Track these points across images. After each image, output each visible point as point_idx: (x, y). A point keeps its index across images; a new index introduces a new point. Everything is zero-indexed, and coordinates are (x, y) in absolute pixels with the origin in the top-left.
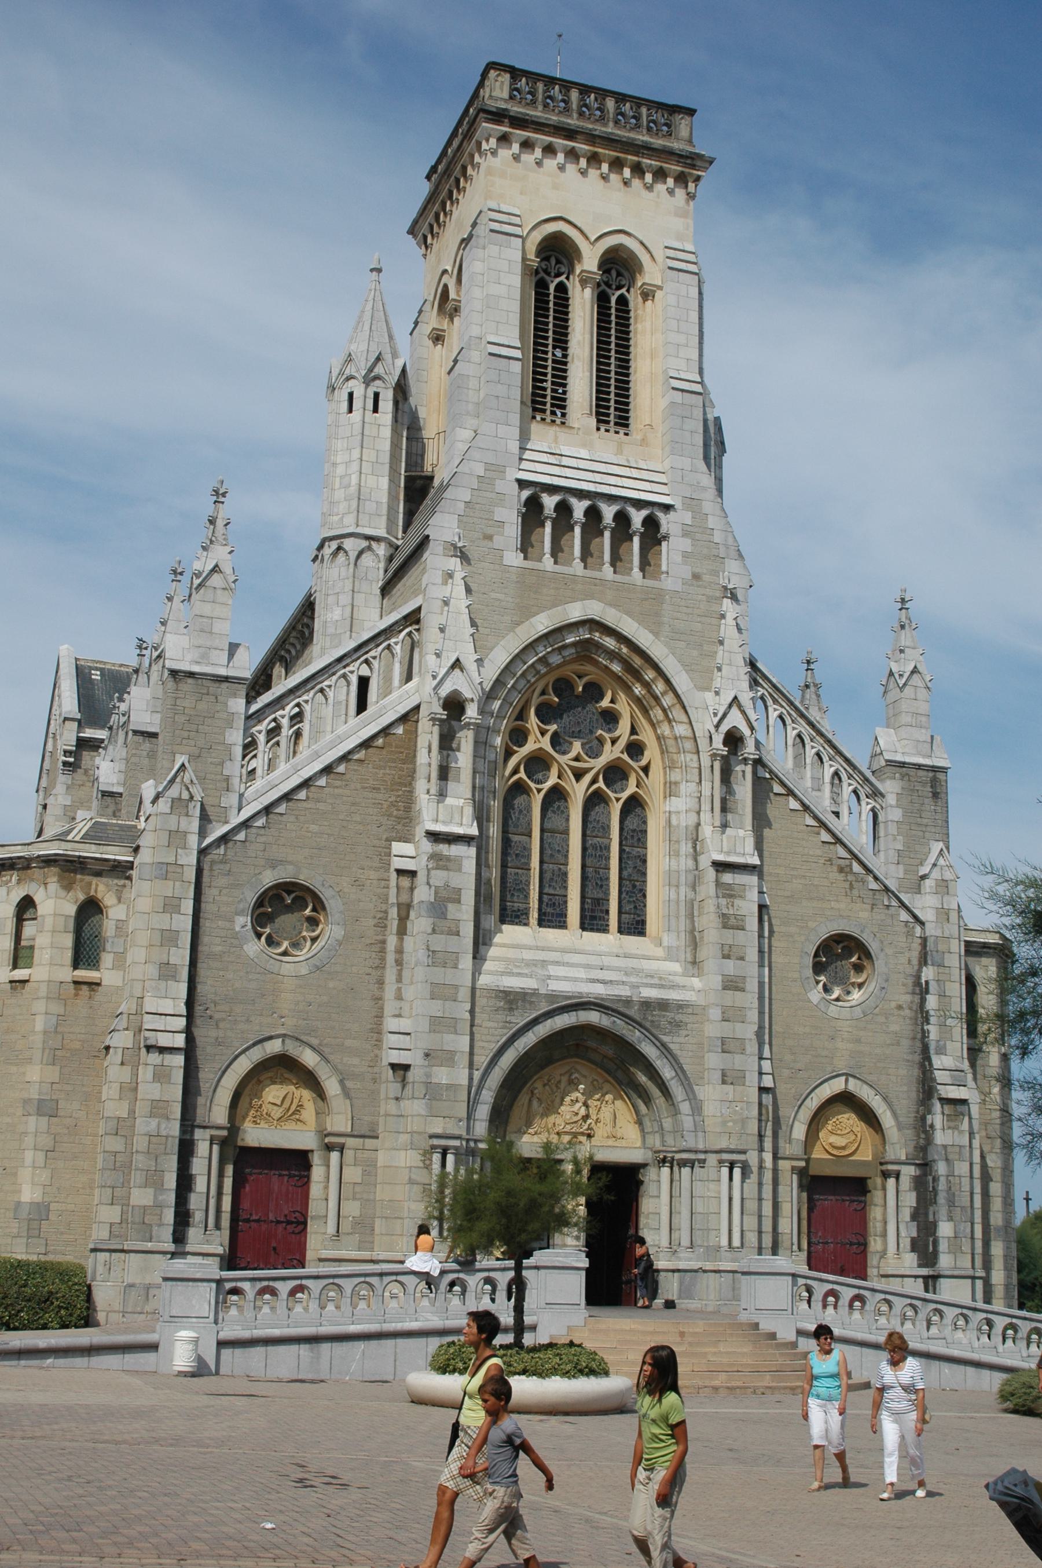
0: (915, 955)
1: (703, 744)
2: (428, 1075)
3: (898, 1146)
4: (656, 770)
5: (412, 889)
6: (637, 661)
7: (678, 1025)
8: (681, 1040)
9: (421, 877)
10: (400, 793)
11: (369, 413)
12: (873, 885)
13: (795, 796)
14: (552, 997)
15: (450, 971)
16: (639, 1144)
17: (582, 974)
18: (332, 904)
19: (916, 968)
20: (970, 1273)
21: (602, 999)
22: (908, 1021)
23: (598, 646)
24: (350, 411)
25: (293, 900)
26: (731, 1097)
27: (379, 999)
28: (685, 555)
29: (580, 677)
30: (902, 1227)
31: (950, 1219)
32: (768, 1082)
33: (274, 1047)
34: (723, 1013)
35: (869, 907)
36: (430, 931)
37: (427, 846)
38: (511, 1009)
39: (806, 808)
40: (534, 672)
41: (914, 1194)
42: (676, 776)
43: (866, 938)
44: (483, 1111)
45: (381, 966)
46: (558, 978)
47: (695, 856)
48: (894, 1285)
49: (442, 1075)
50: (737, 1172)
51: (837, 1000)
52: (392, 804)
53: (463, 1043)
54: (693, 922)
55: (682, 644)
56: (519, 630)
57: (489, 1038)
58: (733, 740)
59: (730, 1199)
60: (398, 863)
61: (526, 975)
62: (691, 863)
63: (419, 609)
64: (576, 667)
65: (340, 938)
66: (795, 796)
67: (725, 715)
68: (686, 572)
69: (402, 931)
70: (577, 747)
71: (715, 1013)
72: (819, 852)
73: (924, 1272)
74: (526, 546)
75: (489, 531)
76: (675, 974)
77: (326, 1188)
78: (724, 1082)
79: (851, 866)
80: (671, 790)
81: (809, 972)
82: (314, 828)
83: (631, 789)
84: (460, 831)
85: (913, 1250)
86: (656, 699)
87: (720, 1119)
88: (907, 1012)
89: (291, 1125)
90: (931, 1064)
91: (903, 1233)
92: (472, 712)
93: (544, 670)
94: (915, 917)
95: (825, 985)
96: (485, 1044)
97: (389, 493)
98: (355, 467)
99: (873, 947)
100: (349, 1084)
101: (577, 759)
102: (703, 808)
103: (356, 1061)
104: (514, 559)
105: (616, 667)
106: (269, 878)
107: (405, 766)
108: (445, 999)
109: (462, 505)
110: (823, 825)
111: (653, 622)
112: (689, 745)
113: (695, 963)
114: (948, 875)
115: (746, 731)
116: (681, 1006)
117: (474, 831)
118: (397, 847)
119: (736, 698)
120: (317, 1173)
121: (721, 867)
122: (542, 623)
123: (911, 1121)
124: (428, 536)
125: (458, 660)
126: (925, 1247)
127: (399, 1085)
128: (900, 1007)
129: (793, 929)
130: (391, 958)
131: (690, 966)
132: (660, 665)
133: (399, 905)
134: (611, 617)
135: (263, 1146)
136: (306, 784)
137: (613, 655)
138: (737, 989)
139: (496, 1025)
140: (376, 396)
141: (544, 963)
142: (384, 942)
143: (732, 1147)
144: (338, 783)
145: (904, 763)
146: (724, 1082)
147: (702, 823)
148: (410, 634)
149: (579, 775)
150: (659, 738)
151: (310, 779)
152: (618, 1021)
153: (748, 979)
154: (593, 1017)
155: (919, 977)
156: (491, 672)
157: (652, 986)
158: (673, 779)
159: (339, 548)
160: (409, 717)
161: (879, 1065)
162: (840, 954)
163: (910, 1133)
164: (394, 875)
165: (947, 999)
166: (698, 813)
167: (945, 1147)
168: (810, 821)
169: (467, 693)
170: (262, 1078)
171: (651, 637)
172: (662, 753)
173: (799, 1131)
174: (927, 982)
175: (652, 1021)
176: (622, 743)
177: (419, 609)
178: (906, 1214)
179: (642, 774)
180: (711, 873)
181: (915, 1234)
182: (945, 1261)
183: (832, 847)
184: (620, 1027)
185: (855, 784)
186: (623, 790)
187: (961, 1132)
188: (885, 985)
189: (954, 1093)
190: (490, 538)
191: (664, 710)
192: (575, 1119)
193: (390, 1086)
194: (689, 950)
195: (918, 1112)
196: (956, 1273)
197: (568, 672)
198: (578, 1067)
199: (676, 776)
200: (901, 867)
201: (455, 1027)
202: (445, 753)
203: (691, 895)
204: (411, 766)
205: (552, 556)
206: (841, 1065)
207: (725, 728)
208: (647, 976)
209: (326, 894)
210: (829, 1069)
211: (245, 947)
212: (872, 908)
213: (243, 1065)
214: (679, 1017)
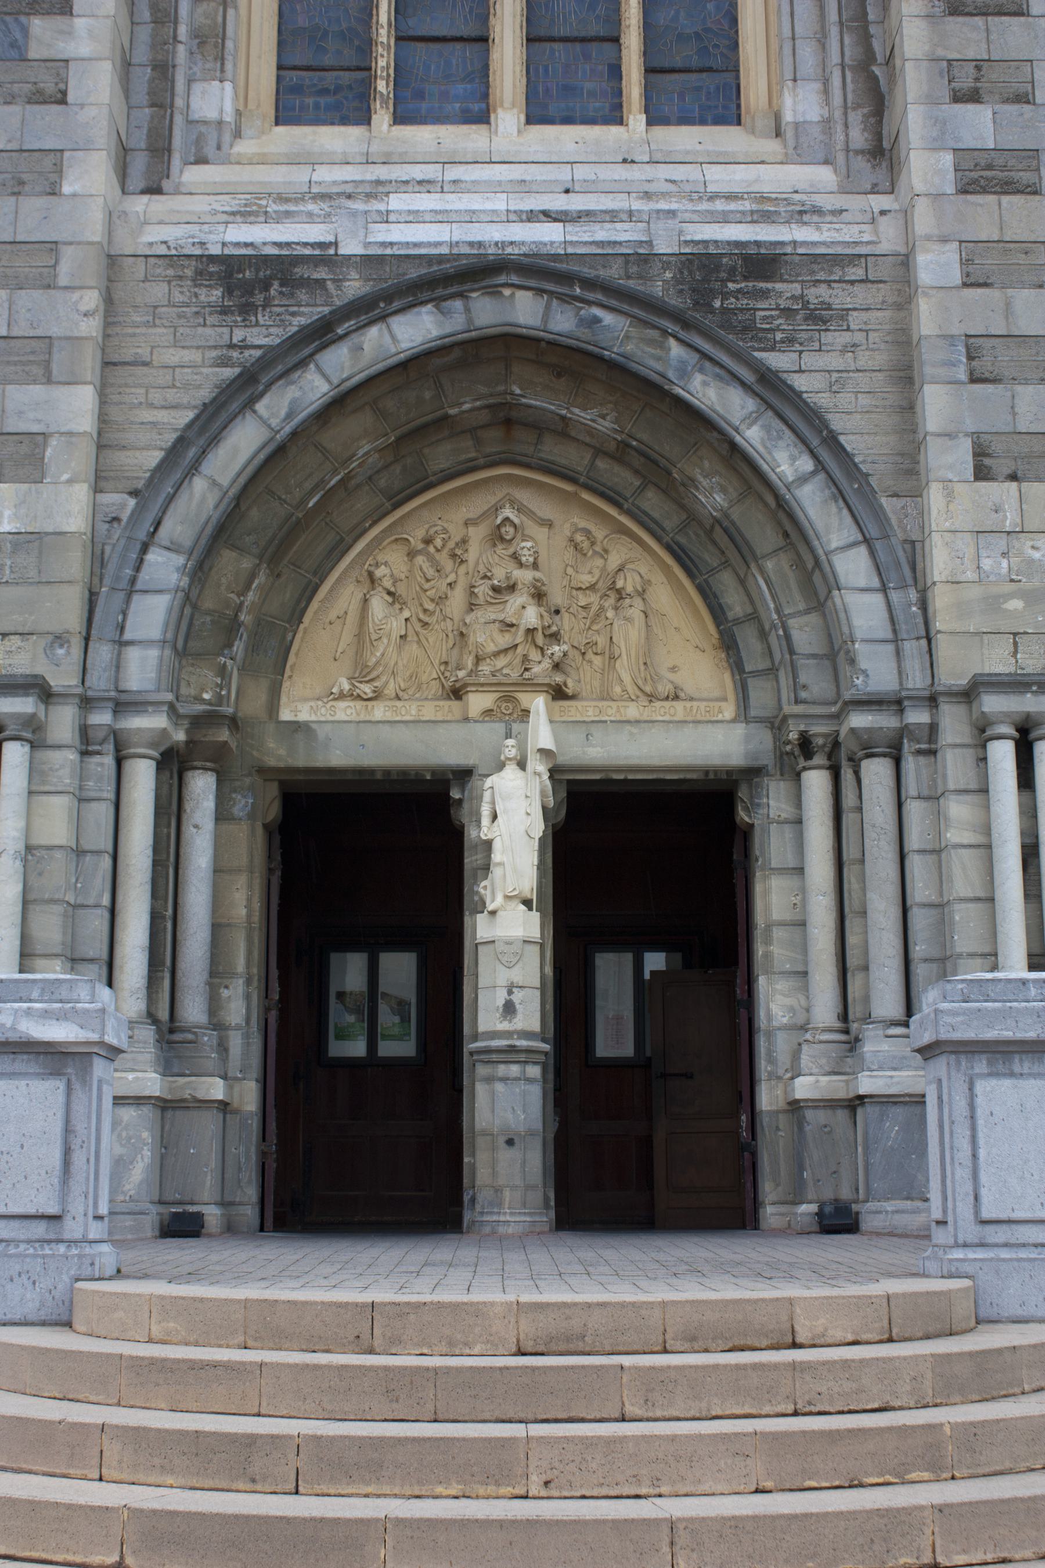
7: (819, 317)
15: (33, 205)
21: (555, 257)
26: (1010, 520)
34: (966, 262)
38: (247, 309)
44: (151, 616)
46: (415, 217)
53: (76, 407)
54: (865, 39)
57: (171, 395)
78: (982, 473)
87: (974, 593)
131: (861, 163)
139: (195, 356)
141: (378, 189)
146: (982, 473)
152: (608, 318)
154: (524, 309)
175: (724, 310)
194: (856, 118)
201: (47, 365)
214: (817, 294)
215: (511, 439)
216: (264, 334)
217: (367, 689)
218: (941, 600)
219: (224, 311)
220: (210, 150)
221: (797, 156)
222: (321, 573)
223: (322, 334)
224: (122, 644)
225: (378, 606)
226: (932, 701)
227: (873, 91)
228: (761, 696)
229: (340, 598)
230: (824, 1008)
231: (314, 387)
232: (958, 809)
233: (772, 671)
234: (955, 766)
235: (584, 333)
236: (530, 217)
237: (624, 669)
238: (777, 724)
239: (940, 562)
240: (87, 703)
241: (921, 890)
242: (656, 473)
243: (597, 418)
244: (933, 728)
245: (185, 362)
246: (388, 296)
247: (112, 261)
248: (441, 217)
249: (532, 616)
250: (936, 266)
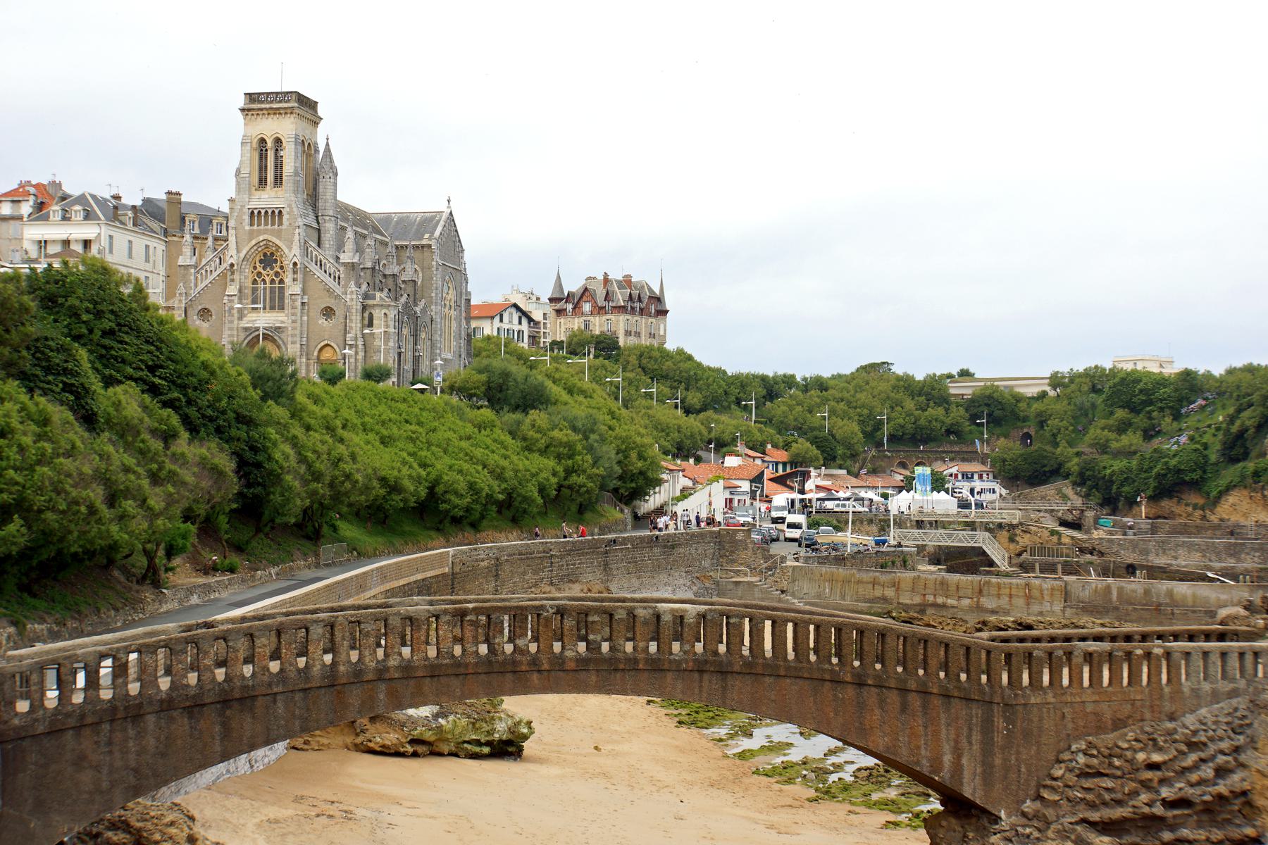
74: (252, 224)
104: (247, 228)
111: (279, 237)
122: (254, 242)
134: (270, 238)
245: (242, 335)
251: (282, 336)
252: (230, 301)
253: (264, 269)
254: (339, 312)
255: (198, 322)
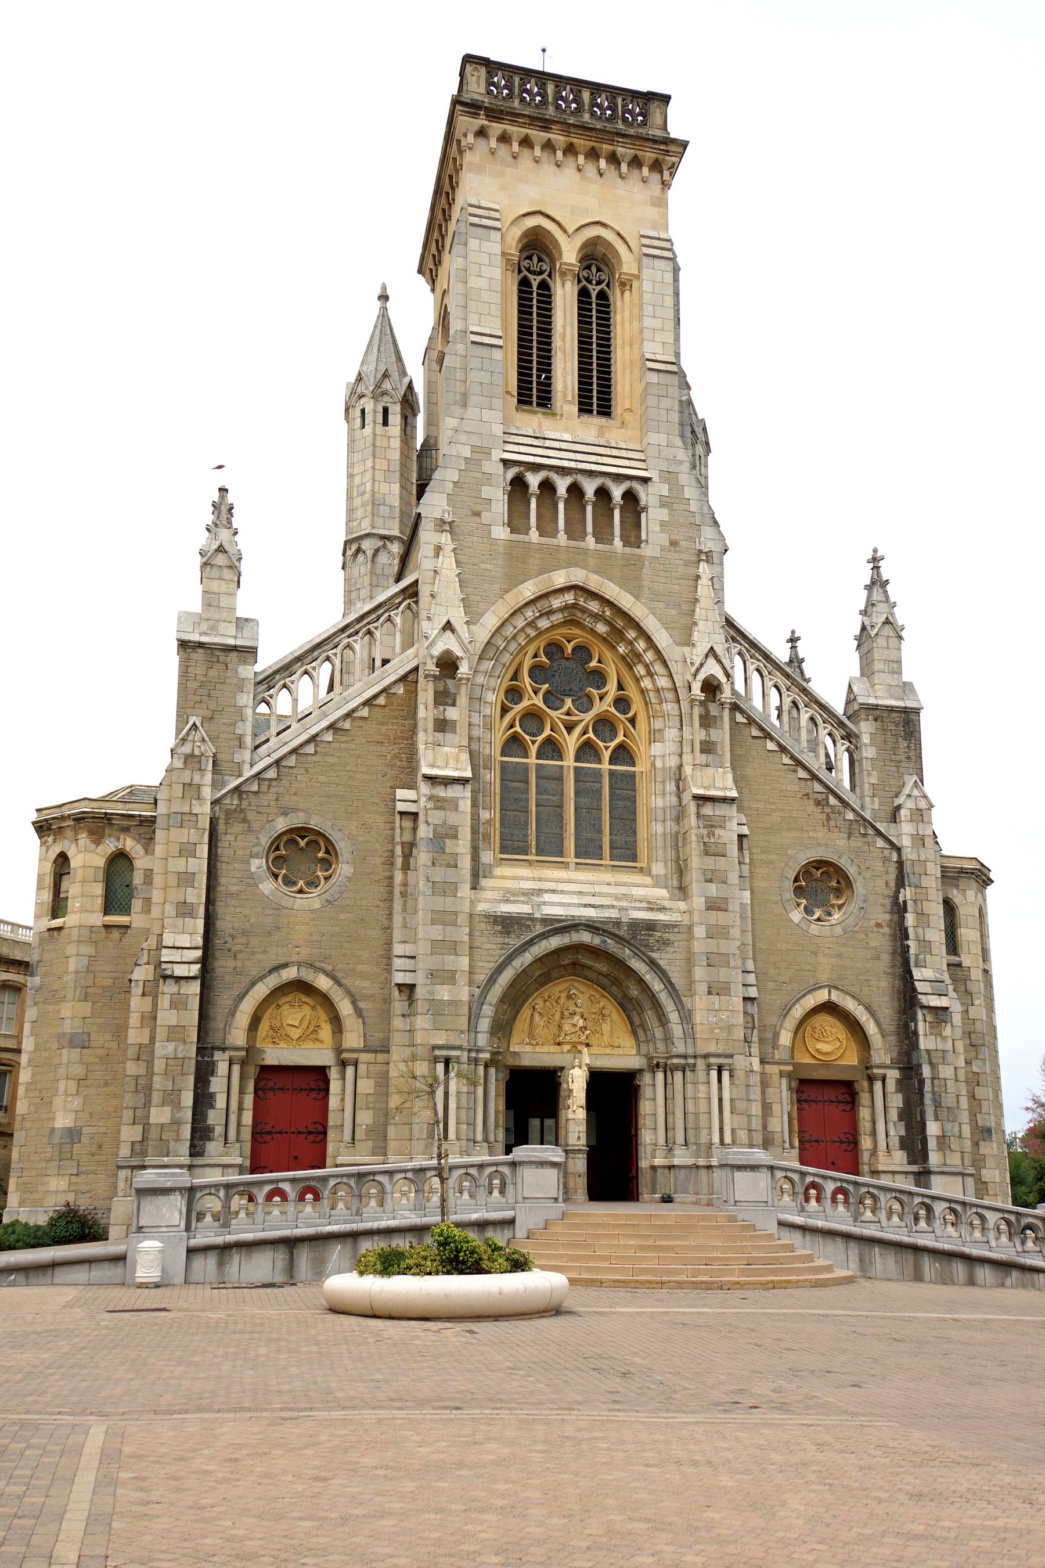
0: (892, 877)
1: (682, 693)
2: (432, 993)
3: (882, 1052)
4: (641, 720)
5: (415, 829)
6: (620, 623)
7: (667, 943)
8: (669, 956)
9: (421, 818)
10: (402, 745)
11: (379, 427)
12: (850, 816)
13: (772, 739)
14: (545, 921)
16: (634, 1052)
17: (575, 900)
18: (342, 846)
19: (893, 889)
20: (960, 1170)
21: (594, 922)
22: (887, 937)
23: (584, 610)
24: (363, 426)
25: (307, 844)
26: (717, 1007)
27: (388, 929)
28: (663, 524)
29: (569, 642)
30: (891, 1125)
31: (937, 1119)
32: (753, 992)
33: (290, 974)
35: (846, 836)
36: (430, 864)
37: (424, 788)
38: (508, 933)
39: (783, 749)
40: (524, 636)
41: (900, 1096)
42: (658, 724)
43: (844, 863)
44: (484, 1024)
45: (390, 898)
46: (553, 904)
47: (679, 794)
48: (885, 1181)
49: (444, 993)
50: (726, 1075)
51: (819, 920)
52: (395, 757)
53: (464, 962)
54: (678, 852)
55: (661, 605)
56: (507, 597)
57: (488, 958)
58: (711, 687)
59: (720, 1100)
60: (400, 807)
61: (523, 902)
62: (674, 801)
63: (417, 582)
64: (564, 630)
65: (350, 875)
66: (772, 739)
67: (702, 665)
68: (664, 539)
69: (406, 867)
70: (569, 703)
71: (700, 932)
72: (796, 788)
73: (914, 1168)
75: (478, 508)
76: (663, 899)
77: (343, 1099)
78: (710, 993)
79: (827, 798)
80: (654, 736)
81: (789, 895)
82: (322, 778)
83: (620, 738)
84: (455, 774)
85: (902, 1148)
86: (639, 656)
88: (886, 930)
89: (309, 1045)
90: (912, 976)
91: (892, 1133)
92: (464, 669)
93: (533, 633)
94: (891, 843)
95: (805, 908)
96: (481, 964)
97: (401, 498)
98: (369, 475)
99: (851, 871)
100: (361, 1005)
101: (568, 714)
102: (685, 750)
103: (367, 984)
104: (501, 532)
105: (601, 628)
106: (281, 824)
107: (407, 722)
108: (445, 924)
109: (451, 485)
110: (799, 763)
111: (632, 584)
112: (670, 695)
113: (682, 890)
114: (923, 804)
115: (723, 679)
116: (668, 926)
117: (468, 774)
118: (401, 793)
119: (712, 648)
120: (335, 1086)
121: (702, 800)
122: (529, 590)
123: (893, 1028)
124: (420, 514)
125: (448, 622)
126: (915, 1145)
127: (407, 1003)
128: (879, 925)
129: (773, 857)
130: (397, 890)
131: (676, 891)
132: (642, 624)
133: (403, 844)
134: (594, 582)
135: (283, 1064)
136: (313, 739)
137: (598, 617)
138: (719, 909)
139: (494, 946)
140: (386, 411)
141: (540, 892)
142: (391, 878)
143: (719, 1051)
144: (345, 738)
145: (877, 705)
146: (710, 993)
147: (684, 764)
148: (409, 607)
149: (570, 728)
150: (643, 692)
151: (317, 735)
152: (609, 941)
153: (730, 901)
155: (897, 898)
156: (483, 630)
157: (639, 909)
158: (656, 727)
159: (359, 550)
160: (409, 678)
161: (860, 977)
162: (822, 882)
163: (893, 1039)
164: (398, 817)
165: (925, 918)
166: (681, 755)
167: (928, 1051)
168: (786, 760)
169: (458, 652)
170: (280, 1003)
171: (632, 599)
172: (646, 704)
173: (785, 1038)
174: (905, 902)
176: (610, 698)
177: (417, 582)
178: (894, 1114)
179: (628, 724)
180: (692, 807)
181: (903, 1133)
182: (934, 1158)
183: (809, 783)
184: (611, 945)
185: (830, 727)
186: (612, 740)
187: (944, 1038)
188: (864, 905)
189: (935, 1002)
190: (478, 514)
191: (647, 666)
192: (573, 1030)
193: (399, 1005)
194: (675, 877)
195: (900, 1020)
196: (946, 1169)
197: (558, 635)
198: (576, 984)
199: (658, 724)
200: (876, 799)
201: (455, 949)
202: (442, 708)
203: (675, 828)
204: (411, 722)
205: (537, 529)
206: (824, 977)
207: (701, 676)
208: (635, 901)
209: (334, 836)
210: (812, 982)
211: (260, 886)
212: (849, 837)
213: (261, 991)
214: (666, 936)
215: (576, 969)
216: (515, 942)
217: (534, 1042)
218: (698, 1029)
219: (502, 933)
220: (487, 874)
221: (656, 885)
222: (521, 1006)
223: (531, 942)
224: (476, 1032)
225: (537, 1017)
226: (695, 1057)
227: (681, 870)
228: (644, 1048)
229: (525, 1013)
230: (661, 1140)
231: (528, 958)
232: (702, 1088)
233: (647, 1041)
234: (701, 1075)
235: (603, 945)
236: (585, 906)
237: (605, 1038)
238: (650, 1058)
239: (699, 1017)
240: (470, 1051)
241: (691, 1108)
242: (616, 982)
243: (602, 967)
244: (695, 1064)
245: (492, 949)
246: (549, 931)
247: (471, 915)
248: (561, 904)
249: (581, 1023)
250: (700, 932)
251: (662, 958)
252: (439, 803)
253: (552, 699)
254: (871, 883)
255: (268, 886)
